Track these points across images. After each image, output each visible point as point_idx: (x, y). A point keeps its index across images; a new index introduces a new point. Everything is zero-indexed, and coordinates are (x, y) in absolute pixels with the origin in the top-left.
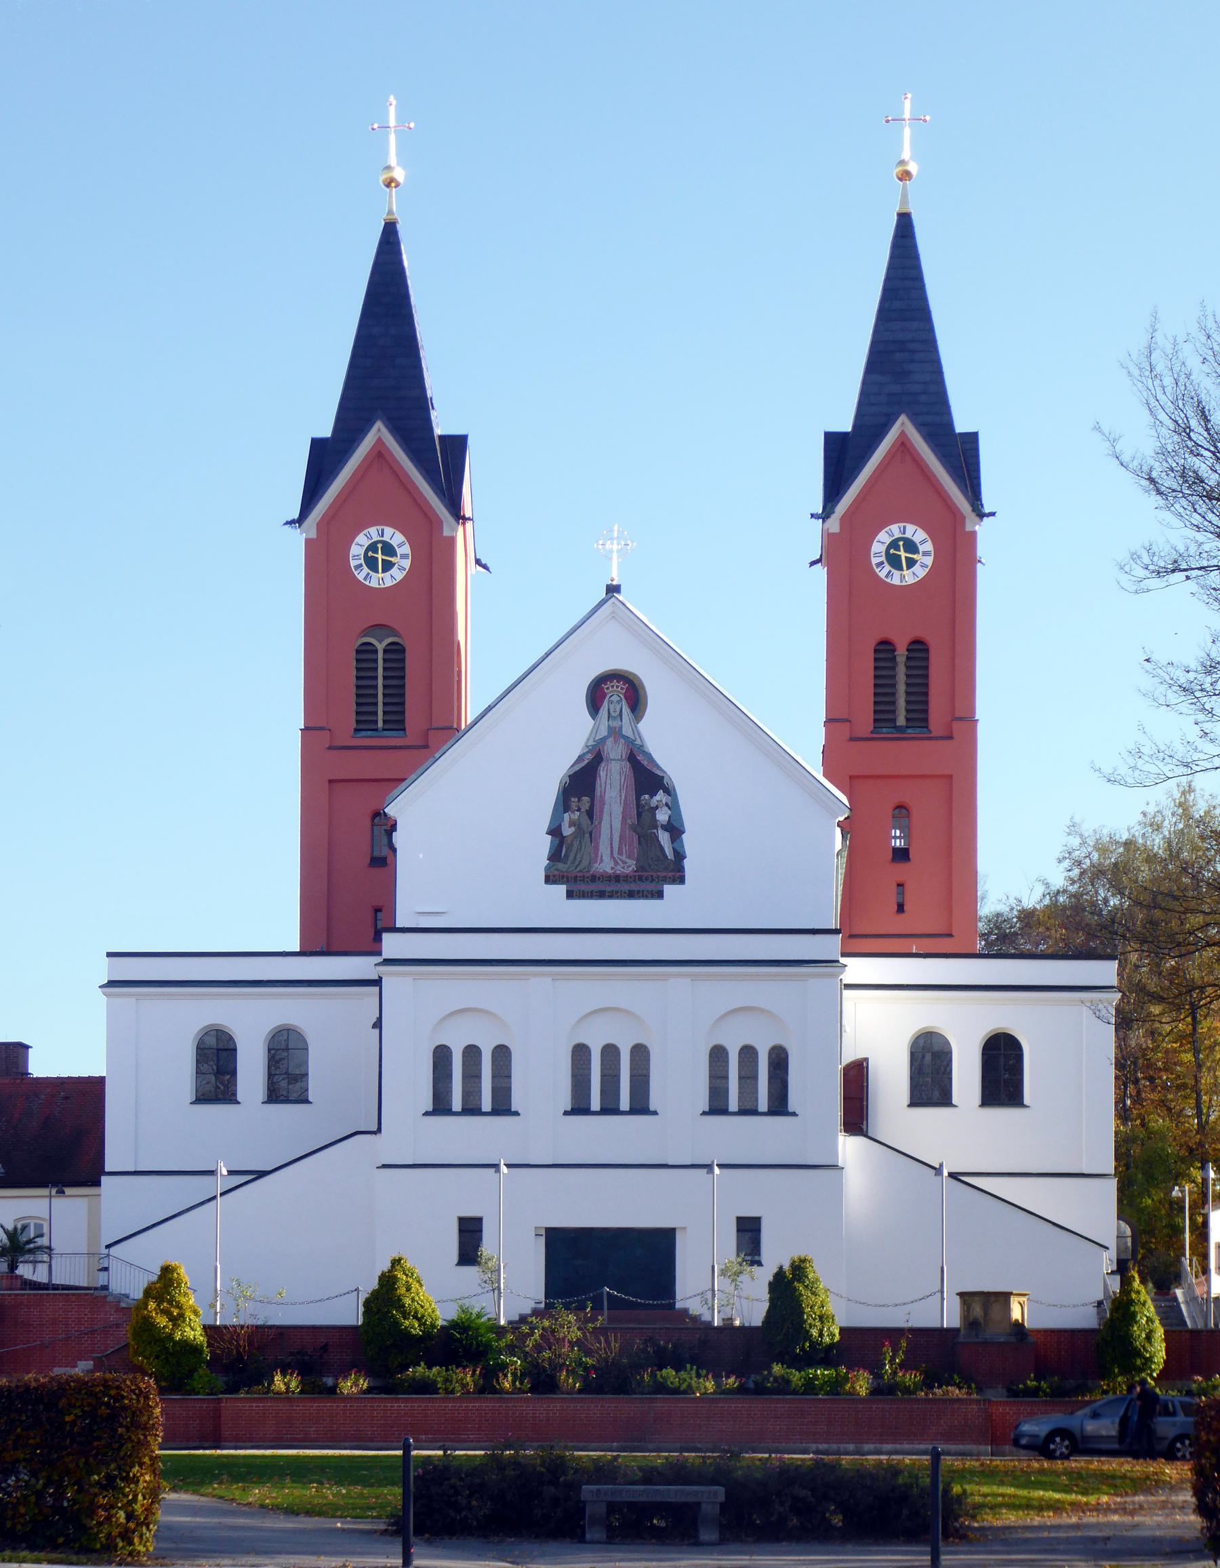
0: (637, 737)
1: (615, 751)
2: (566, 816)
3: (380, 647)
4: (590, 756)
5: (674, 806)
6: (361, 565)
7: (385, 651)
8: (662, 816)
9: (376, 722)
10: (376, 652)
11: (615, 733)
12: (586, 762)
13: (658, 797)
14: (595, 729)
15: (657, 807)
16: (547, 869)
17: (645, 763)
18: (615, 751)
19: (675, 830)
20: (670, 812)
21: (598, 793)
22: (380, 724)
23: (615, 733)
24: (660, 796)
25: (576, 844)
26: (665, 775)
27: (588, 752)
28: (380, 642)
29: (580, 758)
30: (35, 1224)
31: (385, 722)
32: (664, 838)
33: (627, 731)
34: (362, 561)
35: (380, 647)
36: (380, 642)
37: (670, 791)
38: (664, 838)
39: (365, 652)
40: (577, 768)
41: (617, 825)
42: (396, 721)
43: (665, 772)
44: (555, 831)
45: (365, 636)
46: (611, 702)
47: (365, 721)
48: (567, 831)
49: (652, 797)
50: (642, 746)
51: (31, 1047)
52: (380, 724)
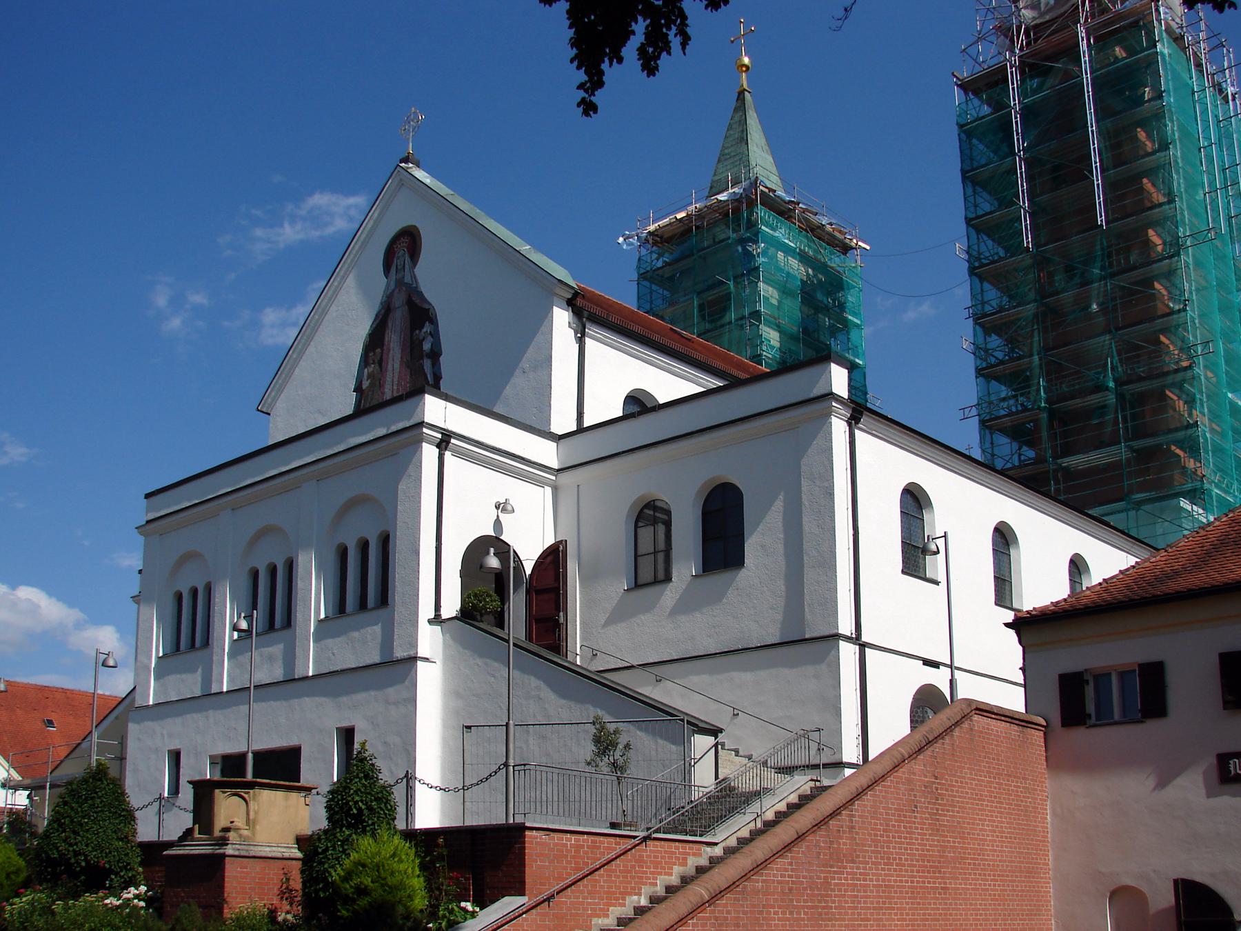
0: (414, 282)
1: (399, 300)
5: (435, 335)
8: (427, 346)
12: (381, 317)
13: (424, 330)
14: (388, 285)
15: (424, 339)
17: (418, 301)
19: (435, 355)
20: (432, 339)
25: (370, 393)
26: (430, 307)
27: (383, 308)
33: (407, 279)
37: (433, 321)
38: (427, 364)
40: (374, 326)
41: (397, 366)
43: (430, 304)
46: (398, 258)
49: (421, 331)
50: (416, 287)
51: (1007, 625)
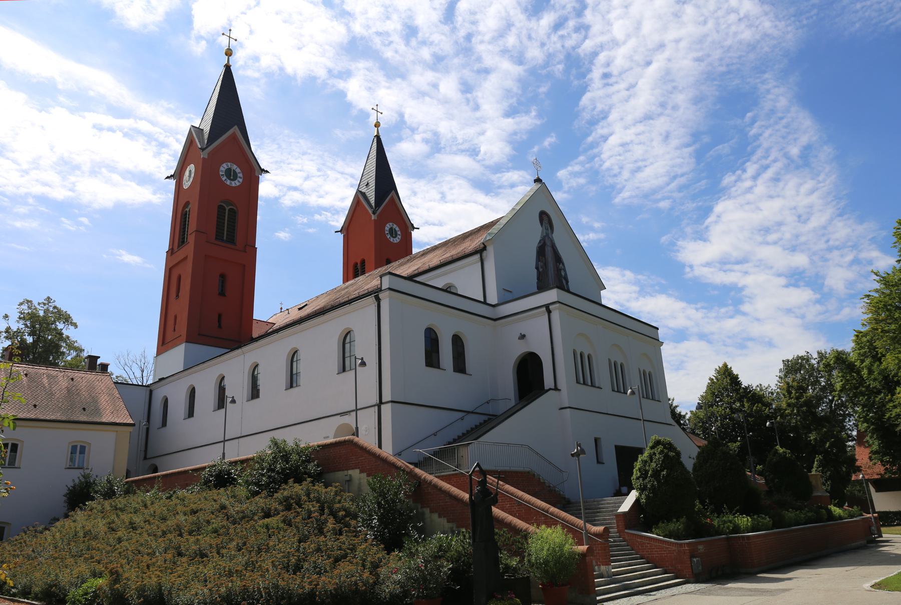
2: (539, 263)
3: (227, 209)
4: (542, 242)
5: (565, 270)
6: (223, 175)
7: (229, 210)
8: (563, 274)
9: (223, 237)
10: (225, 210)
11: (547, 235)
14: (542, 232)
16: (537, 283)
18: (548, 243)
19: (567, 282)
21: (546, 257)
22: (225, 238)
23: (547, 235)
24: (561, 265)
28: (227, 207)
29: (540, 241)
30: (81, 446)
31: (227, 238)
32: (564, 282)
33: (550, 236)
34: (224, 173)
35: (227, 209)
36: (227, 207)
37: (563, 264)
38: (564, 282)
39: (221, 209)
40: (540, 244)
42: (231, 240)
44: (537, 268)
45: (221, 202)
47: (219, 236)
48: (541, 270)
52: (225, 238)
